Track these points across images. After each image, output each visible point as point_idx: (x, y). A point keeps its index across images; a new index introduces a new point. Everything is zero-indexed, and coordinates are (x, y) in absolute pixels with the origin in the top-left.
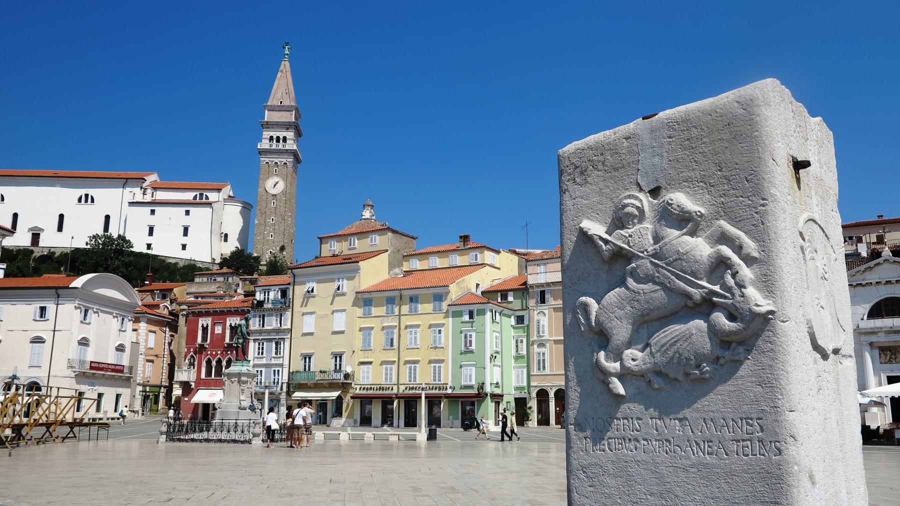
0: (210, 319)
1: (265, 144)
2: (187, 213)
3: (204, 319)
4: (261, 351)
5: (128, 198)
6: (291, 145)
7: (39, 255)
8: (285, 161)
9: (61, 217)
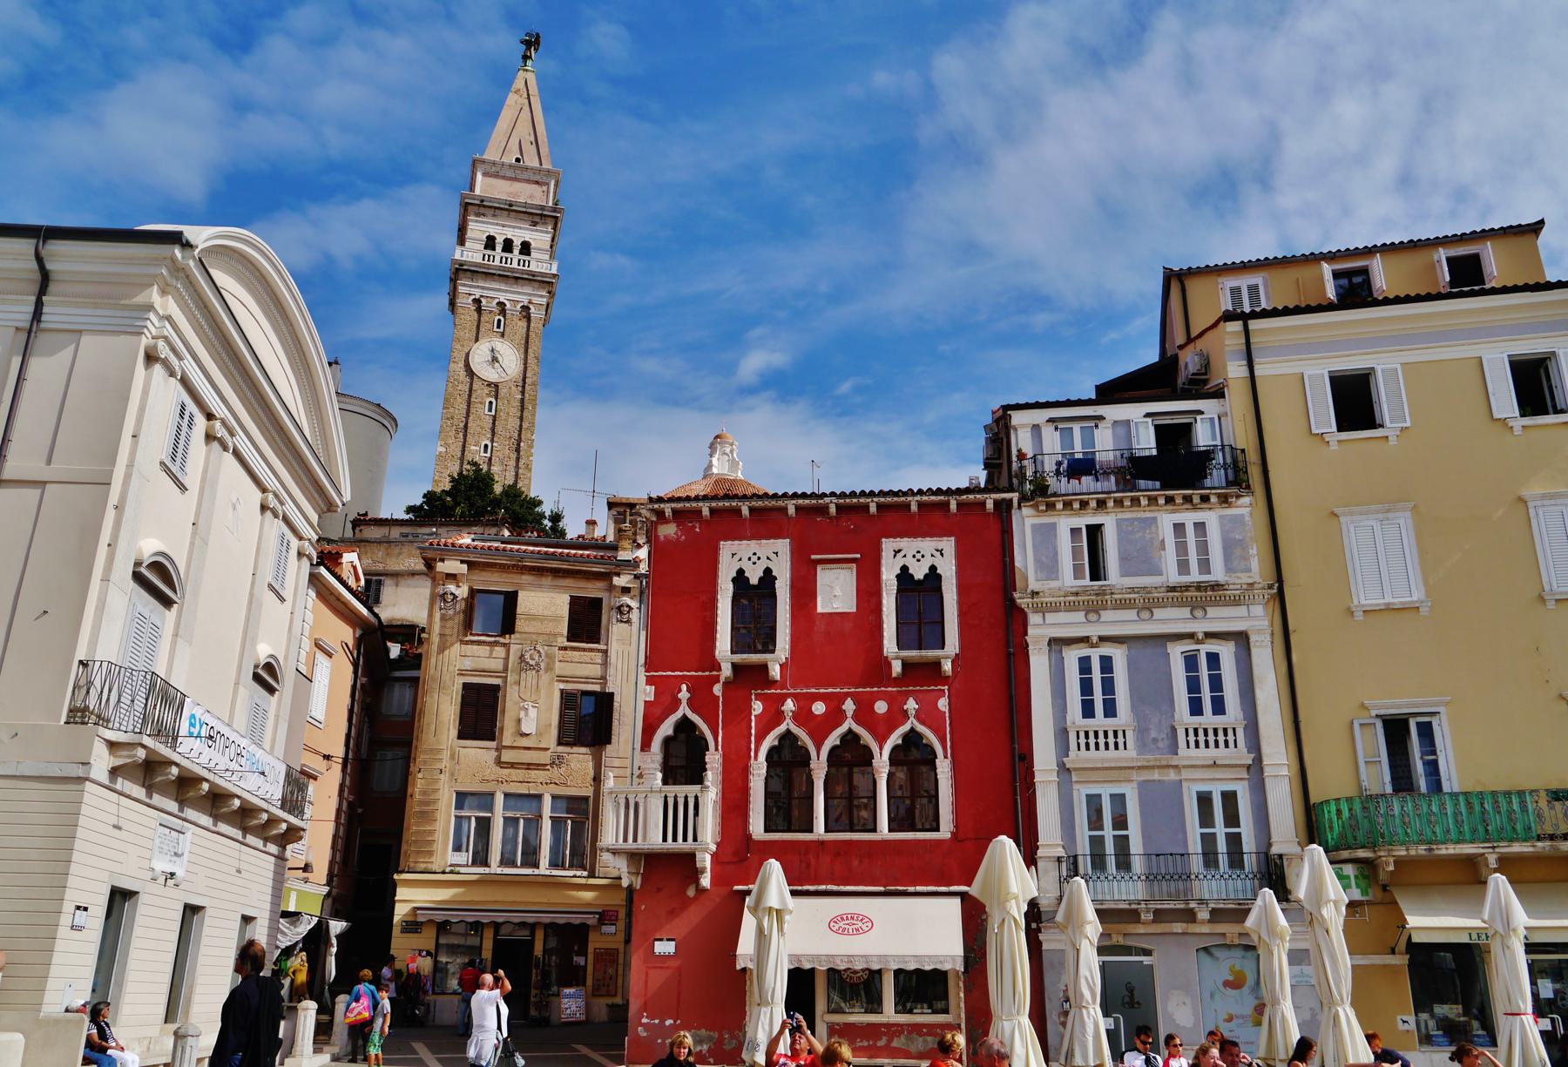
0: (783, 546)
1: (473, 253)
3: (746, 548)
4: (1096, 693)
6: (539, 263)
8: (525, 300)
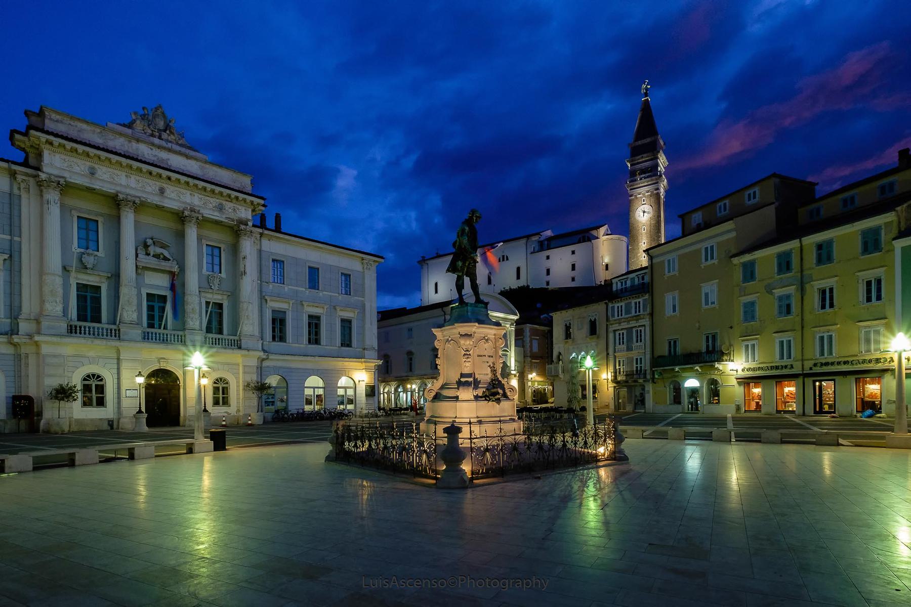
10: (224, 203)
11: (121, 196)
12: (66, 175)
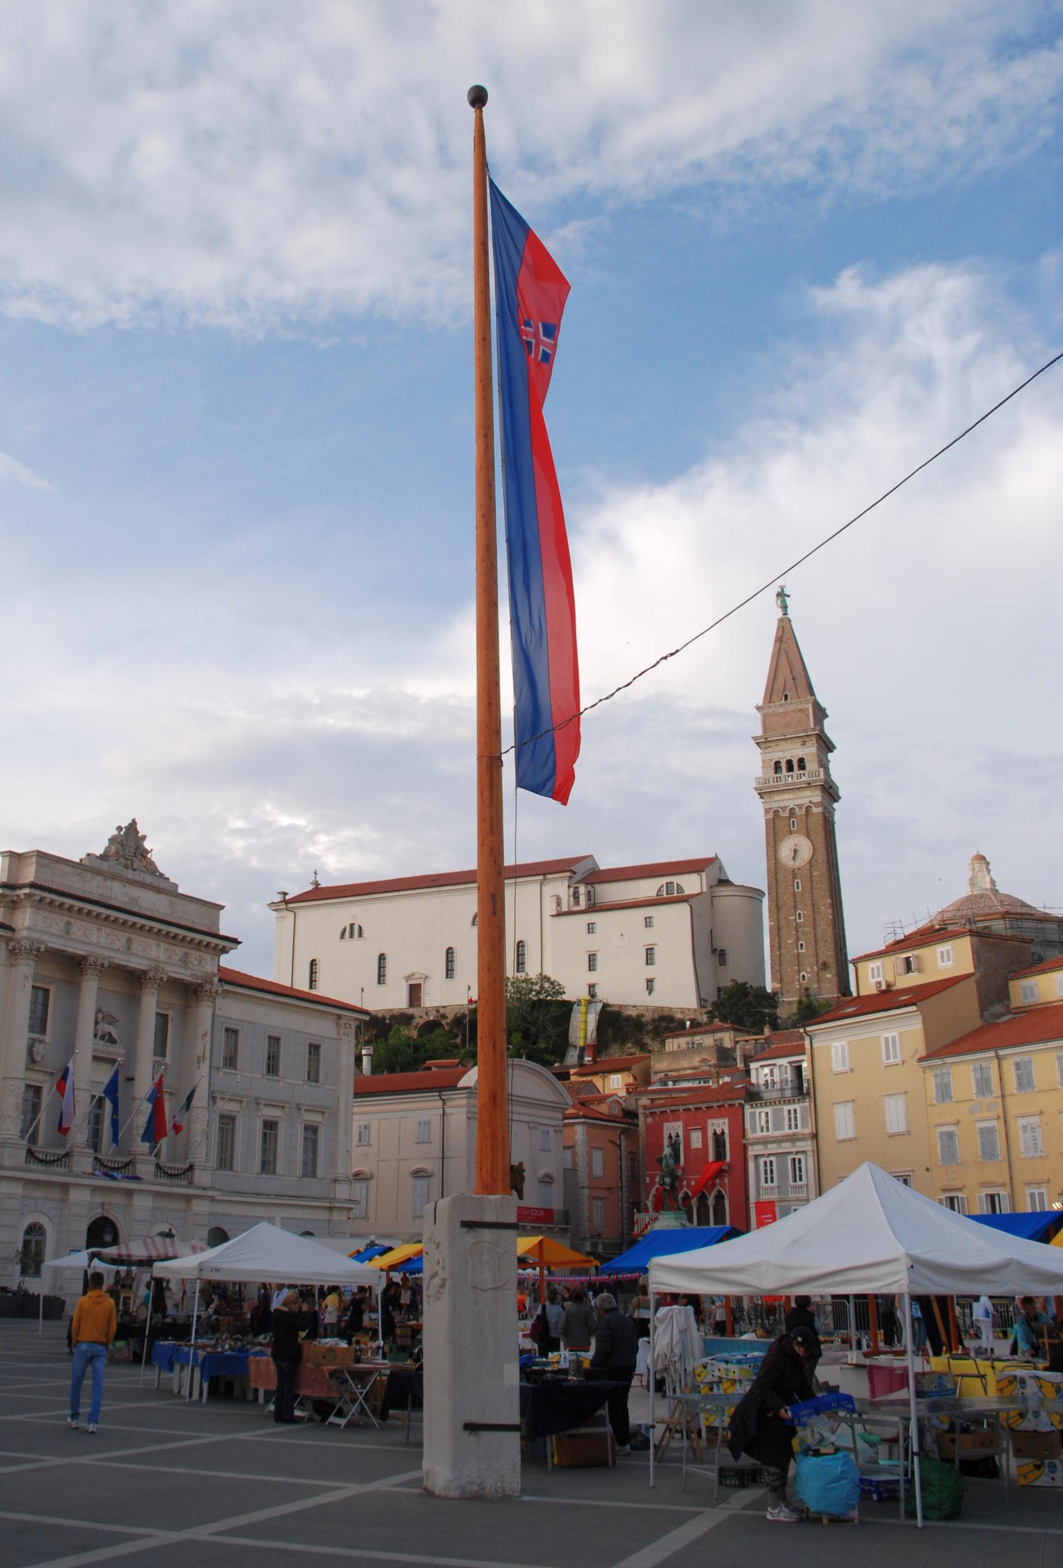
0: (680, 1124)
2: (648, 922)
5: (550, 908)
7: (422, 1021)
9: (450, 952)
10: (189, 951)
11: (92, 959)
12: (45, 938)
